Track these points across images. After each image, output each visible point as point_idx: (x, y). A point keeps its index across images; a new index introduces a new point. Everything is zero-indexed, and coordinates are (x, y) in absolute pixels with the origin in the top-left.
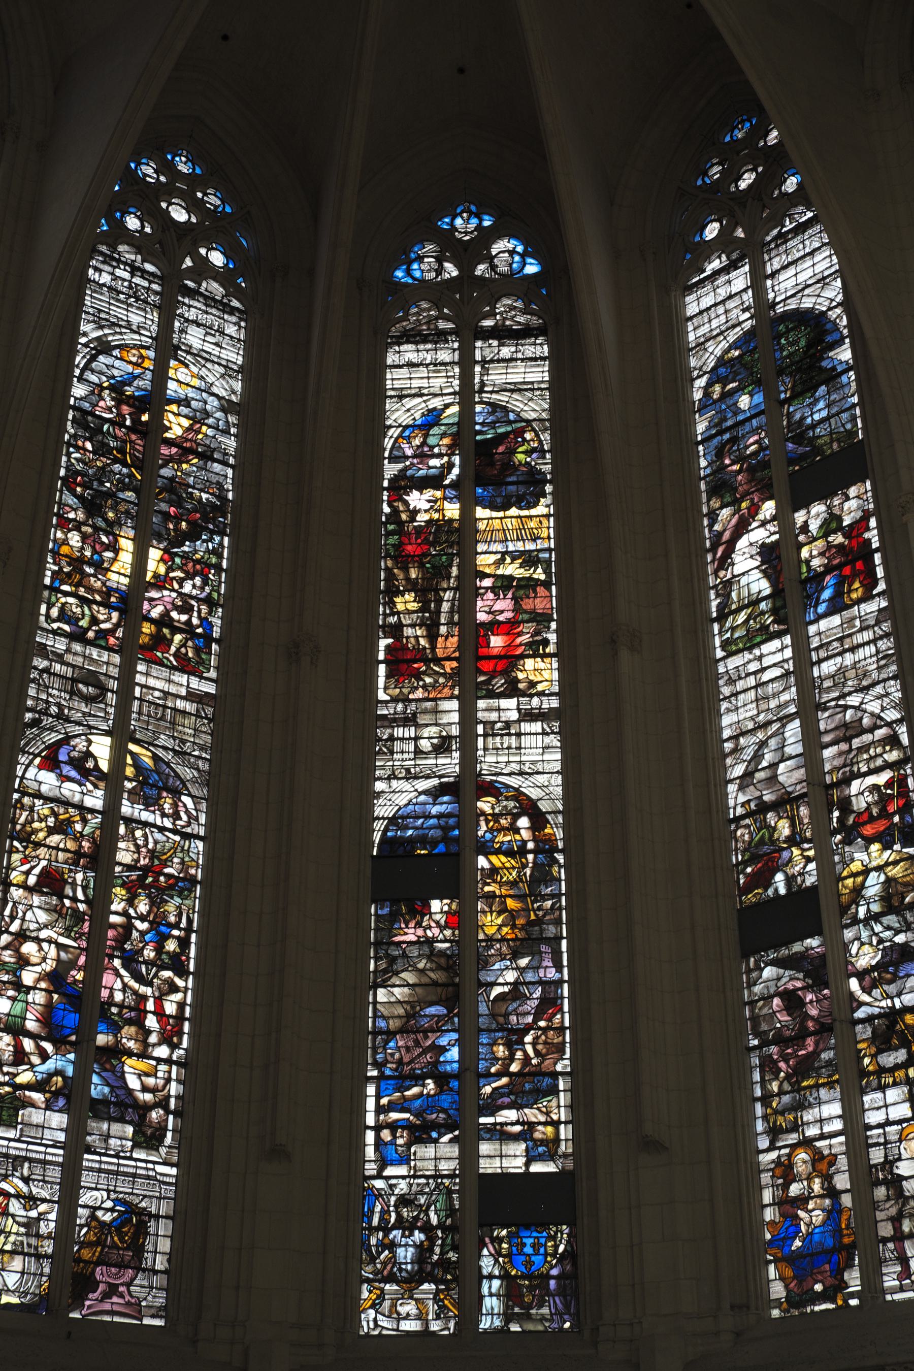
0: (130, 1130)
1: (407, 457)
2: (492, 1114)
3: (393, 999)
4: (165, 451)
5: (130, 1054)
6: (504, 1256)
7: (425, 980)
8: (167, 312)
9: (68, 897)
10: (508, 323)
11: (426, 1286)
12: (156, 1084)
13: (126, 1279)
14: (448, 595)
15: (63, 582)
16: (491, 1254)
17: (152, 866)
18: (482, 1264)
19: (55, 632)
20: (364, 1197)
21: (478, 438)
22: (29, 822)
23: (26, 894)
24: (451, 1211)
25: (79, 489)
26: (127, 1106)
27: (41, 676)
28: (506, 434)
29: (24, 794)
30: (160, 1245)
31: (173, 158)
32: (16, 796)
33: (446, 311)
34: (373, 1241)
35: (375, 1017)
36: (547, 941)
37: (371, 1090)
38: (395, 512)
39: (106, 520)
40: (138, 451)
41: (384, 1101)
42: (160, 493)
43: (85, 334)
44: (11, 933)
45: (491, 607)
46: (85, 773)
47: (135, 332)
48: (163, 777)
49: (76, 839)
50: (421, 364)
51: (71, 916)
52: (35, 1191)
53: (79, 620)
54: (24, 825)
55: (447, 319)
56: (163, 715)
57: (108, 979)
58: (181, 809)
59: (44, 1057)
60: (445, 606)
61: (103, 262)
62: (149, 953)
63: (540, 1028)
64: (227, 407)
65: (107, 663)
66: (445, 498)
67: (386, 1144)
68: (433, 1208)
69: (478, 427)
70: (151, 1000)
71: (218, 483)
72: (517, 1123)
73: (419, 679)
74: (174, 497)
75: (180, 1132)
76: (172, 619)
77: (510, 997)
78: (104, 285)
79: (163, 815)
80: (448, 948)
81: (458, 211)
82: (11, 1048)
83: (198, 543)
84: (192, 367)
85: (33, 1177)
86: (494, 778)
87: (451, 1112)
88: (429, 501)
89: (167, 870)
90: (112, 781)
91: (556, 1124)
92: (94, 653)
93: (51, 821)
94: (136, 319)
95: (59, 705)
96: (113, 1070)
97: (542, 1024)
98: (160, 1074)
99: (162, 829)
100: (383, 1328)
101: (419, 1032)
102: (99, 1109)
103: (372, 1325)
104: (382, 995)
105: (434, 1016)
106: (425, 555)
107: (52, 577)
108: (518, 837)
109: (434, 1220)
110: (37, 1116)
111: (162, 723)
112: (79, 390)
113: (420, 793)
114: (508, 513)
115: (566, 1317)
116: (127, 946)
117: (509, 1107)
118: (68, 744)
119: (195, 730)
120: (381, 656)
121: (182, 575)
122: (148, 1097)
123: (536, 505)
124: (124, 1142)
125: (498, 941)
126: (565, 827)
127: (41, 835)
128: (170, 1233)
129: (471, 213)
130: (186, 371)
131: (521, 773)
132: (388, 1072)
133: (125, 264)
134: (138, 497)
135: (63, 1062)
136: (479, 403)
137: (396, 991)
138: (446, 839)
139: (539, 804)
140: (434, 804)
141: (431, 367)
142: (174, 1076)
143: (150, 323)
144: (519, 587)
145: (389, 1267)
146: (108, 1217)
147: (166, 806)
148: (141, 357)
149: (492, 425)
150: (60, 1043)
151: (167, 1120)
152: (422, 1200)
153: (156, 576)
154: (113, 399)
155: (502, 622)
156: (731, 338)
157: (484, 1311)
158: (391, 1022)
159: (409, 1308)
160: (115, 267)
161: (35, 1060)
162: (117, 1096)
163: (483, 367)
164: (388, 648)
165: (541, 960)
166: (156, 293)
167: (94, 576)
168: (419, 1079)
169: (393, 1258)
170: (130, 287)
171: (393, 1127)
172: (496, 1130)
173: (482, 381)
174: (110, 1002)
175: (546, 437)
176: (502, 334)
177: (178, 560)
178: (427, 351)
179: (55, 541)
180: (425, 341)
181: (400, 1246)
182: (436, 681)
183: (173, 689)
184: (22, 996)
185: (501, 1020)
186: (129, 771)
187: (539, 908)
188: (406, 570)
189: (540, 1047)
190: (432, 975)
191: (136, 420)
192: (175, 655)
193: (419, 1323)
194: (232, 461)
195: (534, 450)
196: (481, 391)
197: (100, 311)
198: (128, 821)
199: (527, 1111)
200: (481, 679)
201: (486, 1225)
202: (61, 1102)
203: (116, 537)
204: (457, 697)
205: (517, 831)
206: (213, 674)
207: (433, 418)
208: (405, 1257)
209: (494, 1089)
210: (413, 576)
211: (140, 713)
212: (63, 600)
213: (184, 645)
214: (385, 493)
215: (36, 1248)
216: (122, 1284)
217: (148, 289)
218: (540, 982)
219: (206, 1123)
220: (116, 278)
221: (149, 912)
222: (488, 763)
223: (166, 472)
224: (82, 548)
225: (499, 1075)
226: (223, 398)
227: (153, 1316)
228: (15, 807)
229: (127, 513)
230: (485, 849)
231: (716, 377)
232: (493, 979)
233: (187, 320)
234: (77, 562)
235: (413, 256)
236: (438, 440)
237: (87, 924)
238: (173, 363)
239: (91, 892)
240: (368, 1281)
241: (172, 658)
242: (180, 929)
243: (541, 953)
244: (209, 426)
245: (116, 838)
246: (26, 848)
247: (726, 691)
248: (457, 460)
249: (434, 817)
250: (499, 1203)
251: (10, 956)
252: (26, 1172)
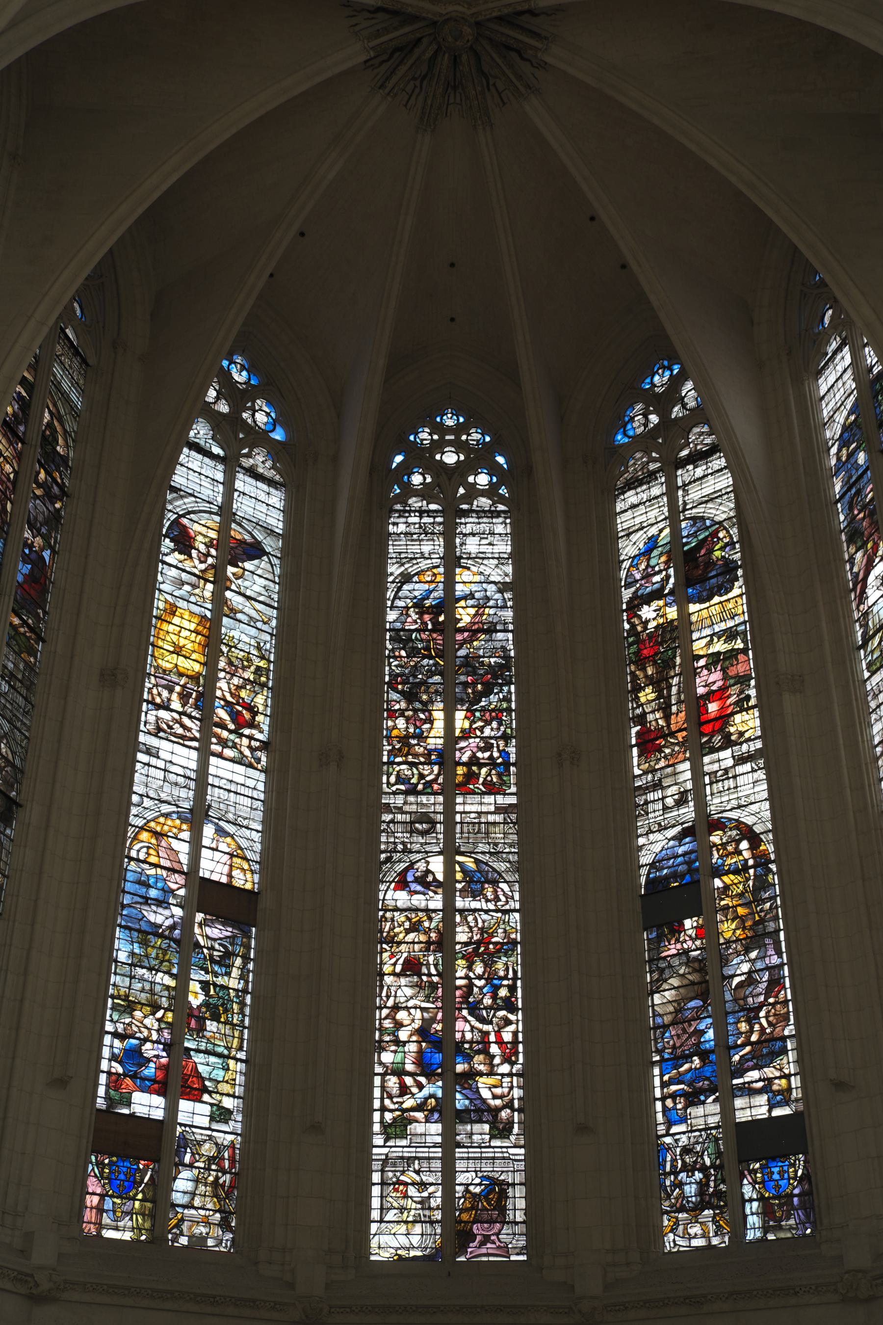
0: (486, 1127)
1: (637, 581)
2: (741, 1076)
3: (665, 1001)
4: (459, 637)
5: (481, 1074)
6: (759, 1183)
7: (686, 982)
8: (449, 534)
9: (424, 975)
10: (699, 447)
11: (706, 1212)
13: (495, 1230)
14: (675, 681)
15: (396, 756)
16: (750, 1183)
17: (483, 939)
18: (744, 1191)
19: (394, 793)
20: (659, 1151)
21: (686, 548)
22: (392, 929)
23: (396, 979)
24: (719, 1154)
25: (400, 687)
26: (483, 1111)
27: (388, 826)
28: (706, 538)
29: (386, 911)
30: (518, 1203)
31: (441, 419)
32: (381, 913)
33: (654, 454)
34: (668, 1183)
35: (654, 1016)
36: (769, 934)
37: (656, 1071)
38: (633, 626)
39: (421, 702)
40: (440, 644)
41: (666, 1078)
42: (459, 670)
43: (392, 574)
44: (388, 1008)
45: (708, 680)
46: (427, 885)
47: (428, 558)
48: (484, 873)
49: (426, 933)
50: (640, 504)
51: (429, 987)
52: (424, 1178)
53: (411, 779)
54: (388, 932)
55: (655, 460)
56: (479, 829)
57: (460, 1025)
58: (500, 893)
60: (674, 690)
61: (398, 517)
62: (487, 1001)
63: (770, 1004)
64: (503, 588)
65: (434, 804)
66: (666, 605)
67: (670, 1110)
68: (706, 1153)
69: (684, 540)
70: (493, 1034)
71: (502, 647)
72: (760, 1080)
73: (661, 752)
74: (470, 669)
76: (478, 759)
77: (746, 984)
78: (401, 533)
79: (487, 901)
80: (699, 955)
81: (655, 370)
82: (397, 1085)
83: (492, 697)
84: (474, 569)
86: (720, 815)
87: (712, 1079)
88: (655, 611)
89: (494, 940)
90: (447, 887)
91: (787, 1077)
92: (424, 799)
93: (407, 925)
94: (426, 548)
95: (403, 843)
96: (470, 1089)
97: (771, 1000)
98: (505, 1085)
99: (487, 912)
100: (680, 1246)
101: (685, 1022)
102: (463, 1116)
103: (672, 1245)
104: (657, 999)
105: (694, 1008)
106: (656, 654)
107: (388, 755)
108: (741, 858)
109: (708, 1162)
111: (479, 835)
112: (392, 616)
113: (669, 840)
114: (713, 602)
115: (807, 1225)
116: (471, 1000)
117: (752, 1069)
118: (413, 868)
119: (504, 834)
120: (634, 741)
121: (482, 724)
122: (498, 1102)
123: (732, 588)
124: (484, 1136)
125: (734, 942)
126: (775, 842)
127: (401, 936)
129: (664, 368)
130: (468, 573)
131: (739, 807)
132: (666, 1056)
133: (415, 511)
134: (443, 678)
135: (435, 1089)
136: (684, 520)
137: (666, 994)
138: (690, 871)
139: (754, 828)
140: (680, 846)
141: (648, 504)
143: (437, 547)
144: (725, 659)
145: (680, 1201)
146: (478, 1190)
147: (489, 894)
148: (435, 575)
149: (695, 535)
150: (430, 1075)
152: (698, 1148)
153: (463, 730)
154: (417, 613)
155: (715, 691)
156: (848, 407)
157: (748, 1227)
158: (665, 1018)
159: (696, 1230)
160: (407, 517)
161: (415, 1090)
162: (475, 1105)
163: (684, 490)
164: (637, 733)
165: (766, 951)
166: (440, 524)
167: (418, 744)
168: (688, 1058)
169: (682, 1196)
170: (420, 527)
171: (673, 1096)
172: (745, 1088)
173: (684, 501)
174: (463, 1041)
175: (734, 531)
176: (696, 458)
177: (478, 714)
178: (643, 491)
179: (387, 728)
180: (641, 485)
181: (686, 1184)
182: (673, 750)
183: (485, 809)
184: (401, 1049)
185: (741, 1002)
186: (459, 876)
187: (761, 910)
188: (644, 669)
189: (771, 1019)
190: (689, 977)
191: (435, 622)
192: (483, 784)
193: (704, 1240)
194: (511, 627)
195: (727, 545)
196: (685, 510)
197: (400, 553)
198: (462, 911)
199: (766, 1070)
200: (704, 739)
201: (744, 1161)
202: (436, 1116)
203: (430, 711)
204: (688, 759)
205: (740, 853)
206: (513, 789)
207: (652, 543)
208: (691, 1192)
209: (741, 1057)
210: (650, 673)
211: (462, 833)
212: (398, 769)
213: (490, 775)
214: (625, 614)
215: (430, 1217)
216: (493, 1235)
217: (433, 523)
218: (767, 968)
219: (543, 1116)
220: (408, 524)
221: (484, 973)
222: (715, 804)
223: (462, 653)
224: (407, 727)
225: (744, 1045)
226: (499, 582)
227: (518, 1254)
228: (381, 921)
229: (437, 692)
230: (718, 872)
231: (844, 442)
232: (733, 972)
233: (465, 535)
234: (404, 739)
235: (627, 419)
236: (658, 560)
237: (440, 990)
238: (458, 570)
239: (440, 967)
240: (667, 1212)
241: (481, 787)
242: (508, 979)
243: (766, 945)
244: (491, 607)
245: (454, 925)
246: (391, 947)
247: (873, 705)
248: (671, 571)
249: (680, 856)
250: (752, 1144)
251: (390, 1023)
252: (417, 1167)
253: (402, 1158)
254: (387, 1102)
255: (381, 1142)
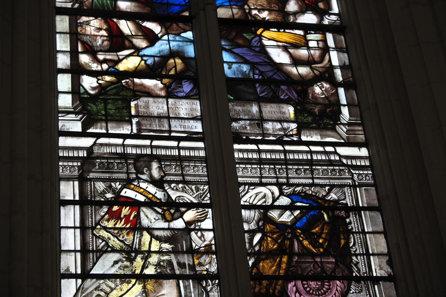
0: (290, 111)
12: (310, 55)
26: (278, 83)
52: (174, 195)
59: (152, 39)
75: (359, 105)
82: (104, 33)
85: (168, 178)
96: (248, 45)
98: (312, 44)
102: (241, 89)
110: (158, 107)
122: (303, 70)
124: (285, 125)
128: (381, 228)
142: (331, 43)
146: (287, 217)
151: (337, 94)
161: (140, 43)
162: (261, 73)
202: (187, 87)
215: (192, 267)
252: (156, 173)
253: (124, 156)
254: (84, 59)
255: (77, 127)
